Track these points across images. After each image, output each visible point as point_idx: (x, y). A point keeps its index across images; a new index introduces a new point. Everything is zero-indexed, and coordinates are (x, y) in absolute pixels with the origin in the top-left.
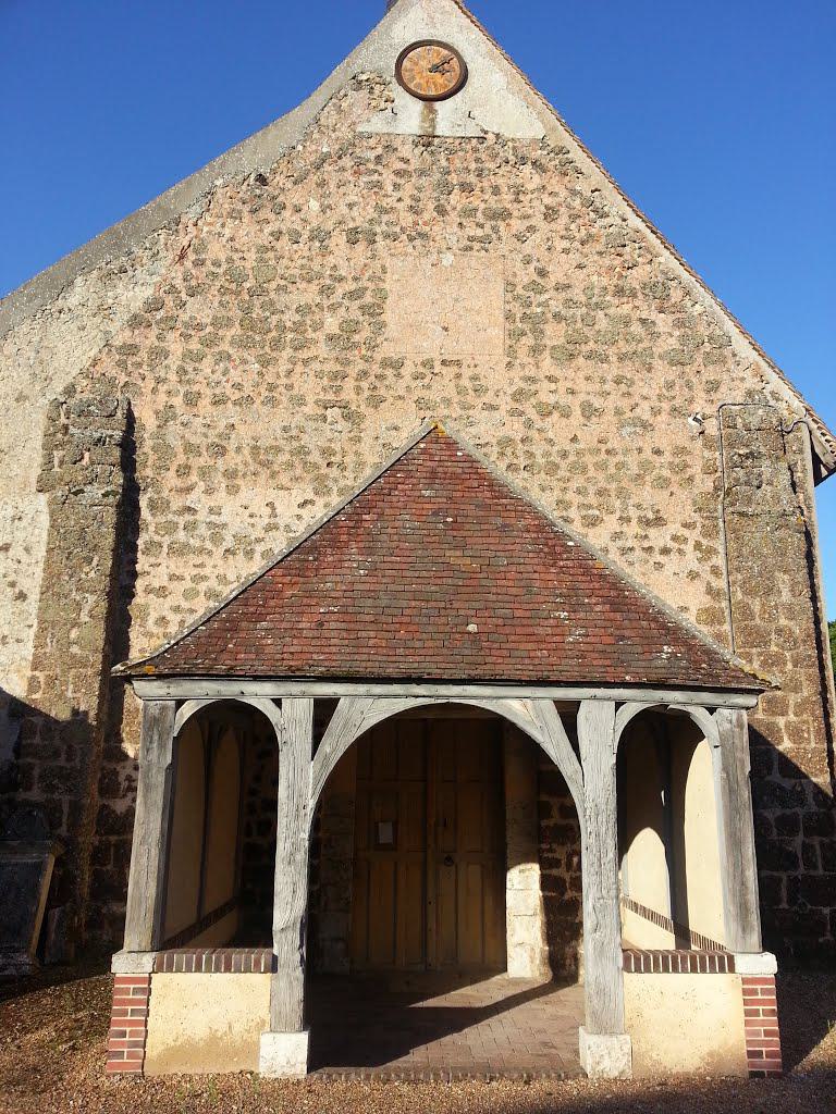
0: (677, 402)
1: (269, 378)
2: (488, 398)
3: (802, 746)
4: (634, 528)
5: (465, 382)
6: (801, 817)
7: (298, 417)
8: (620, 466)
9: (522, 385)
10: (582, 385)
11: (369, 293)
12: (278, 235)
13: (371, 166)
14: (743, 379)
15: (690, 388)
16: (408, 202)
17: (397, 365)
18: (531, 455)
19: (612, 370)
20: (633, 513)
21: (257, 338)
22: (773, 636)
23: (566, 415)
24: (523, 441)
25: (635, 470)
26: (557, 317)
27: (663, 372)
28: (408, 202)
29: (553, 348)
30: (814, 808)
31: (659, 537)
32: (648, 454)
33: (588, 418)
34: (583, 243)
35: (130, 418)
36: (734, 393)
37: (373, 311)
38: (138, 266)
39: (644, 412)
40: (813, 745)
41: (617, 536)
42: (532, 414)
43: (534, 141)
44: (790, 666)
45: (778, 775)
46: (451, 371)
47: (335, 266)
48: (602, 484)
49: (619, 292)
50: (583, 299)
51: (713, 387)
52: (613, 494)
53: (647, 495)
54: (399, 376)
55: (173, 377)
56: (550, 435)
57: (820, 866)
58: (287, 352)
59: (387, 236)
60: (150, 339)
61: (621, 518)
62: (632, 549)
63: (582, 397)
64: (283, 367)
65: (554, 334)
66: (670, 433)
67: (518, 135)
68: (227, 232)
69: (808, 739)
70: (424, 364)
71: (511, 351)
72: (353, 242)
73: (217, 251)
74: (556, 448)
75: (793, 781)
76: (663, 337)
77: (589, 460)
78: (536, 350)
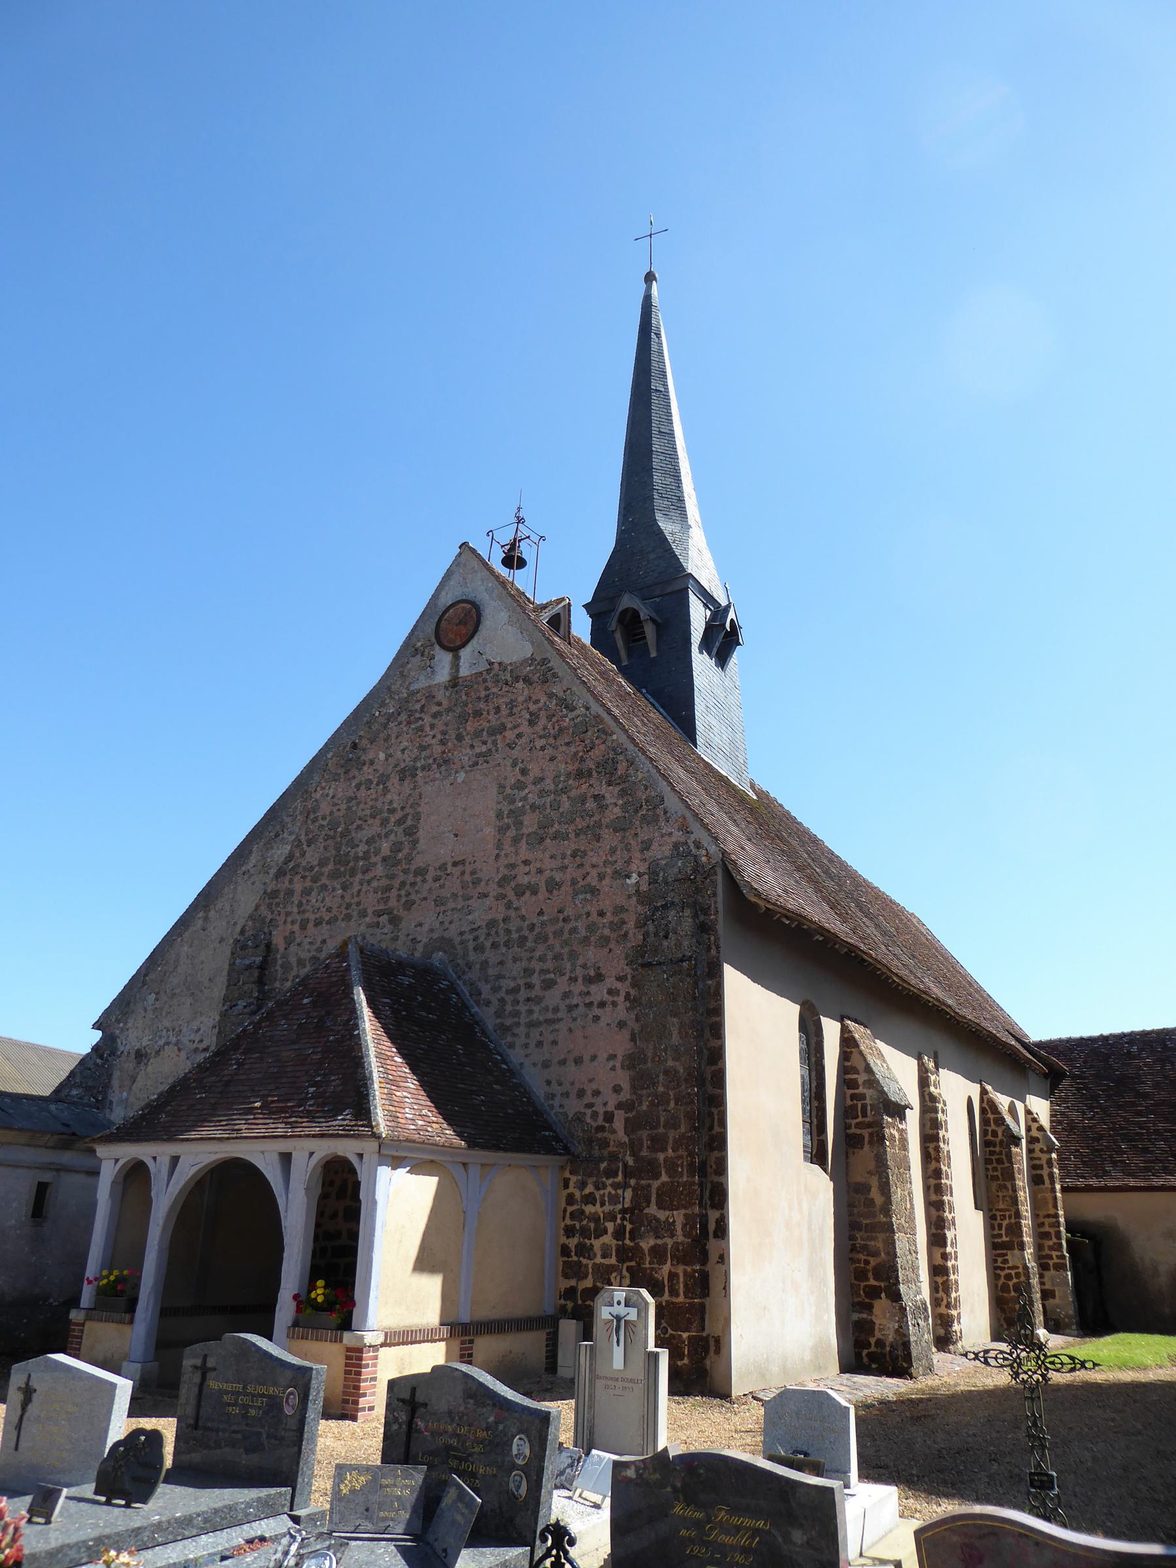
0: (619, 866)
1: (347, 900)
2: (481, 888)
3: (676, 1179)
4: (579, 987)
5: (467, 877)
6: (669, 1246)
7: (362, 928)
8: (574, 930)
9: (506, 872)
10: (548, 864)
11: (410, 817)
12: (358, 787)
13: (418, 715)
14: (671, 834)
15: (628, 850)
16: (439, 737)
17: (421, 872)
18: (508, 931)
19: (569, 846)
20: (579, 972)
21: (342, 869)
22: (661, 1078)
23: (535, 893)
24: (504, 920)
25: (583, 932)
26: (534, 807)
27: (609, 839)
28: (439, 737)
29: (529, 835)
30: (680, 1239)
31: (599, 992)
32: (594, 917)
33: (551, 892)
34: (555, 738)
35: (268, 946)
36: (663, 848)
37: (411, 832)
38: (285, 830)
39: (593, 880)
40: (685, 1179)
41: (566, 995)
42: (511, 895)
43: (526, 660)
44: (672, 1104)
45: (655, 1207)
46: (456, 871)
47: (391, 801)
48: (557, 949)
49: (579, 774)
50: (552, 787)
51: (646, 846)
52: (566, 957)
53: (591, 955)
54: (424, 881)
55: (295, 910)
56: (524, 912)
57: (682, 1294)
58: (359, 876)
59: (423, 768)
60: (285, 884)
61: (570, 978)
62: (577, 1006)
63: (547, 873)
64: (356, 888)
65: (530, 822)
66: (612, 895)
67: (514, 659)
68: (331, 792)
69: (682, 1172)
70: (440, 868)
71: (499, 845)
72: (402, 780)
73: (325, 808)
74: (527, 923)
75: (667, 1213)
76: (610, 807)
77: (550, 929)
78: (516, 841)
